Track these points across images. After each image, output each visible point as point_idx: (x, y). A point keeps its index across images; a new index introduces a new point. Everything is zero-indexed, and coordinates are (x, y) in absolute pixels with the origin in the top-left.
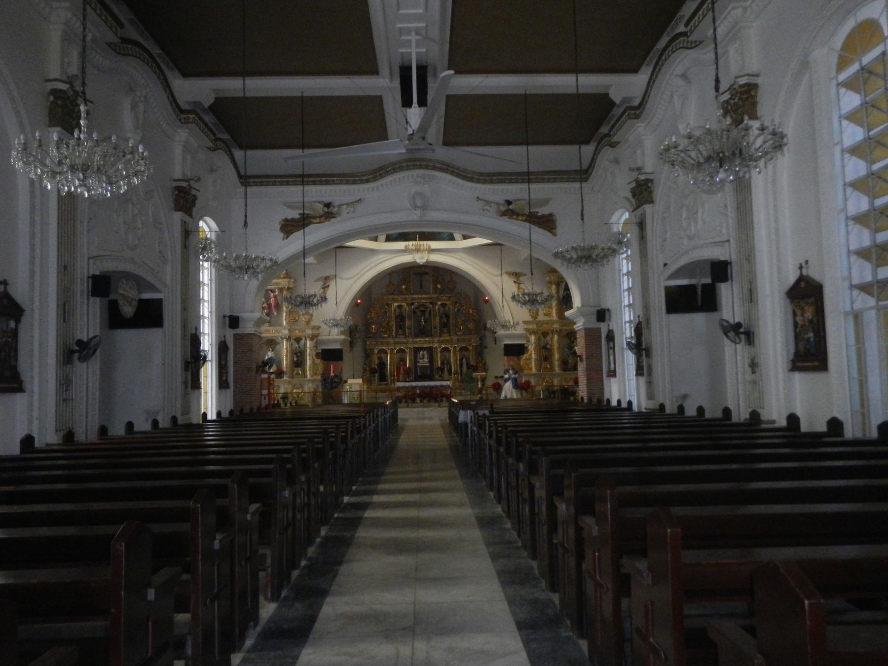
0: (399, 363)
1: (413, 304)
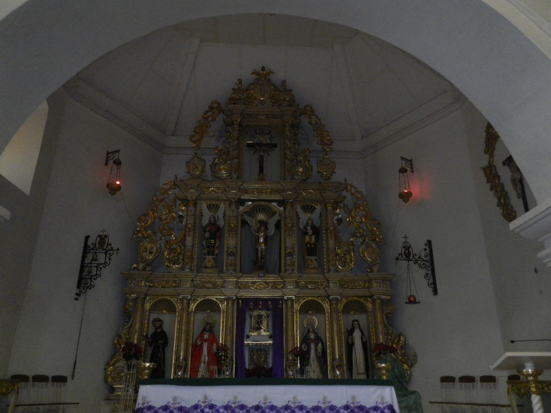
0: (201, 335)
1: (241, 202)
